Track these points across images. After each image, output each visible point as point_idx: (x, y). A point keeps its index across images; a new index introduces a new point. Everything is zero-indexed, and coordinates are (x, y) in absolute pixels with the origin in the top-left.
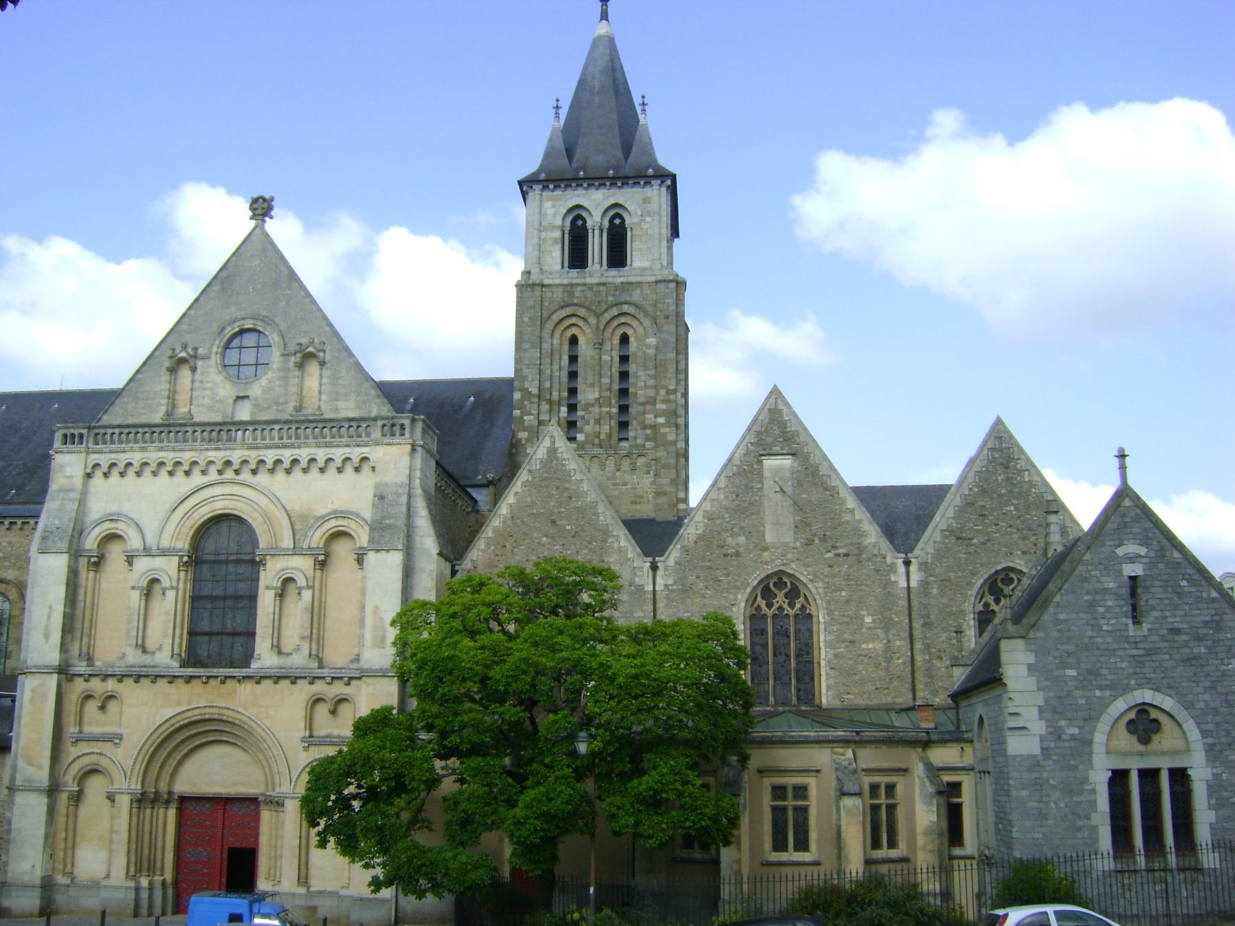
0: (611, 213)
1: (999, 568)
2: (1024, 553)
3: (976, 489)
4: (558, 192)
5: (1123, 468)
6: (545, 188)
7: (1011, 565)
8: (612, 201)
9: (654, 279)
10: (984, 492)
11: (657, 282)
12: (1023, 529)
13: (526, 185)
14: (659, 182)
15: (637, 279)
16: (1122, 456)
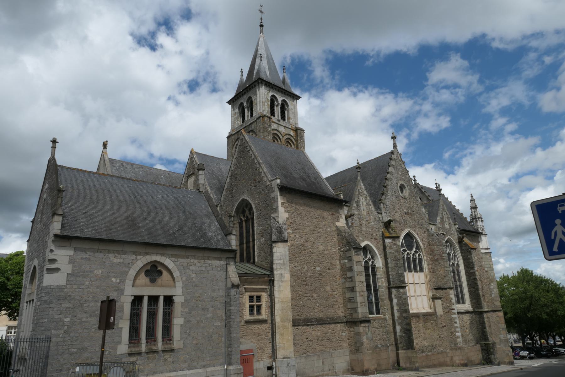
0: (250, 101)
1: (240, 200)
2: (247, 191)
3: (235, 166)
4: (237, 101)
5: (54, 147)
6: (233, 102)
7: (243, 197)
8: (248, 96)
9: (255, 119)
10: (237, 167)
11: (257, 119)
12: (247, 179)
13: (229, 102)
14: (257, 83)
15: (253, 121)
16: (54, 142)
